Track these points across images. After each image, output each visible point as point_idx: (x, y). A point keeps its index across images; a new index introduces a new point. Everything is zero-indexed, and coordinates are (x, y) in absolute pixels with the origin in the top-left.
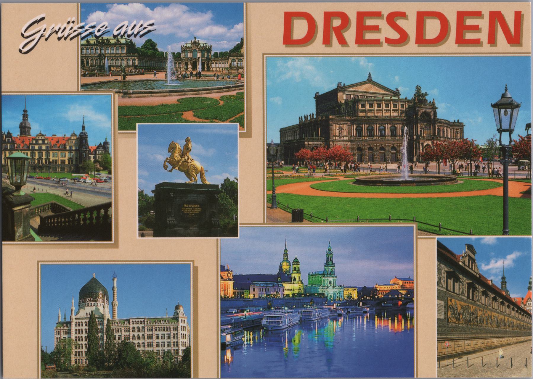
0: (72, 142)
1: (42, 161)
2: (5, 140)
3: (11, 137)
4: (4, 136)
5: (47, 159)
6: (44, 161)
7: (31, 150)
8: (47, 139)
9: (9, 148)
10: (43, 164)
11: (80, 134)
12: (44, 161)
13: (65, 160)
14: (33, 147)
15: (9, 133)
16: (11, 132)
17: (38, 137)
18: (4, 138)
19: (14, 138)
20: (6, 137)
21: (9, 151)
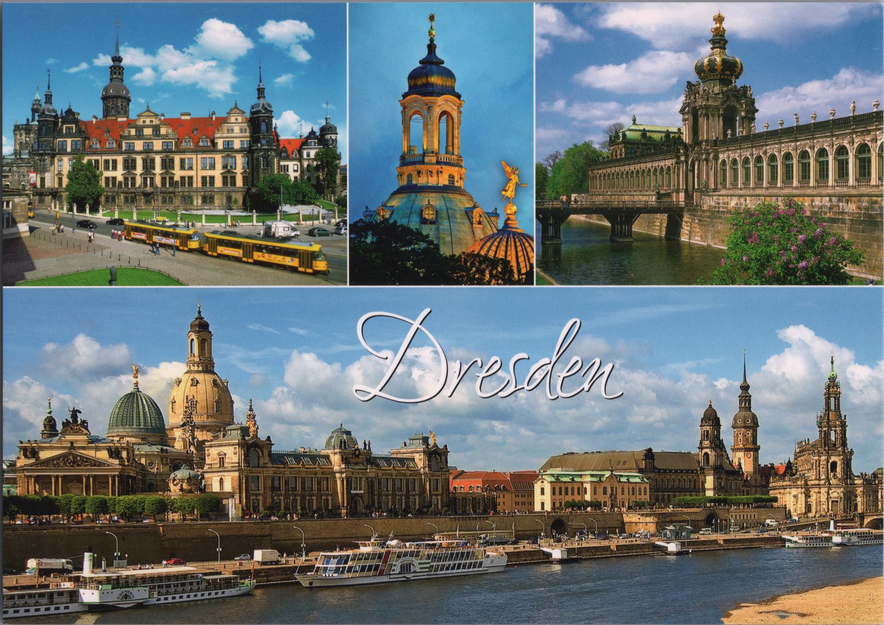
0: (232, 130)
1: (152, 179)
2: (61, 129)
3: (76, 122)
4: (60, 120)
5: (167, 177)
6: (158, 181)
7: (126, 152)
8: (169, 122)
9: (69, 150)
10: (157, 187)
11: (253, 108)
12: (158, 181)
13: (212, 178)
14: (129, 145)
15: (69, 112)
16: (74, 110)
17: (142, 120)
18: (60, 124)
19: (84, 122)
20: (63, 123)
21: (70, 157)
